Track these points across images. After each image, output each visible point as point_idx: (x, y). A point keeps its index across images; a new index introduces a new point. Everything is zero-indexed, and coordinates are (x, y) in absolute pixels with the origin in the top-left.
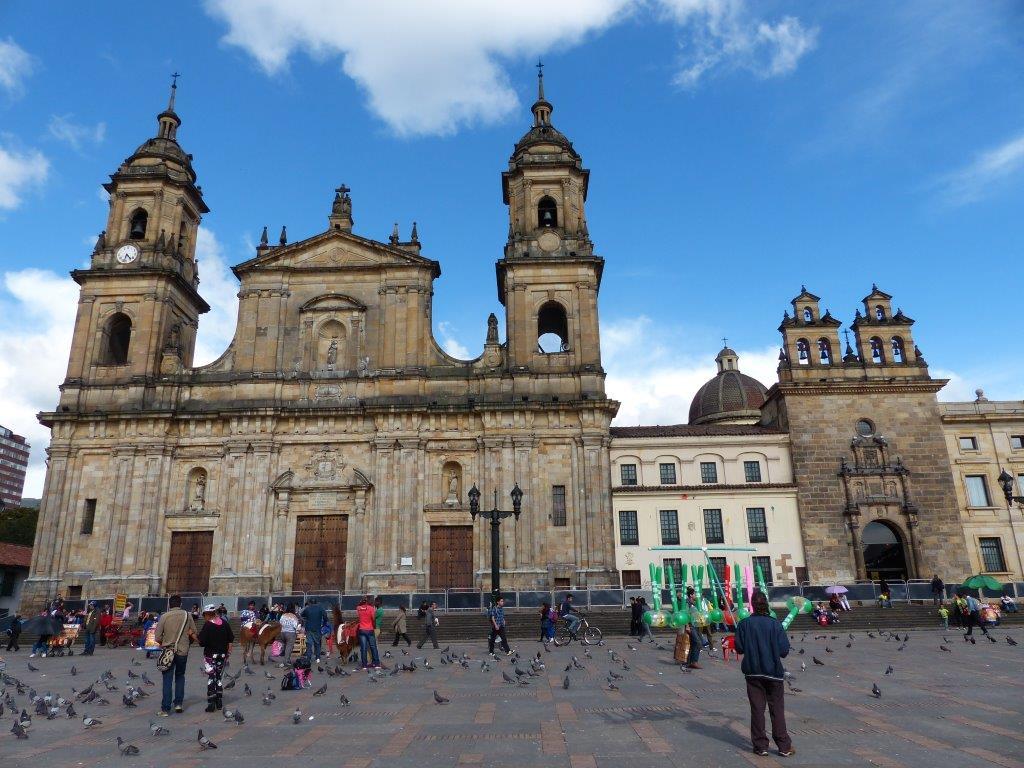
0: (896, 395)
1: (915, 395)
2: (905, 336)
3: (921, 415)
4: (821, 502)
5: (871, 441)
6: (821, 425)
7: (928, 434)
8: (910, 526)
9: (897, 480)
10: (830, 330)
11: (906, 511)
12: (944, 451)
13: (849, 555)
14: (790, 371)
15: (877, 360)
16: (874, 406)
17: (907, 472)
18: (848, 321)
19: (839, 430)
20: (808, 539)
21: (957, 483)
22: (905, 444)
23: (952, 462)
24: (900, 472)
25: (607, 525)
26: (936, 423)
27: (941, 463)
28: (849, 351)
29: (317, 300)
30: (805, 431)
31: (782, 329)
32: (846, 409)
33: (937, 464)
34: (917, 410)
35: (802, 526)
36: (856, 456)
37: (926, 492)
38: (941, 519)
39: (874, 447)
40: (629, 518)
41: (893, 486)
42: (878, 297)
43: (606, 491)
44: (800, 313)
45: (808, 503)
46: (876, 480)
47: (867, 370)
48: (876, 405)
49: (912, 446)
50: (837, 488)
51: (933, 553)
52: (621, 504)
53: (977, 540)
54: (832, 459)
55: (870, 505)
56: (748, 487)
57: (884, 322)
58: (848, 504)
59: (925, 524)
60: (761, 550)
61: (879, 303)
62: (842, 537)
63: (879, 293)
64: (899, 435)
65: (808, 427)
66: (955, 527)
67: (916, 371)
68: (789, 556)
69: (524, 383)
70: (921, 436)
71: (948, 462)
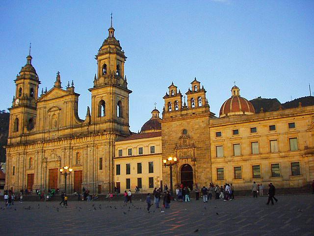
11: (194, 160)
24: (194, 146)
27: (207, 142)
28: (185, 104)
29: (51, 109)
40: (118, 166)
41: (191, 152)
46: (185, 150)
52: (117, 162)
59: (199, 165)
60: (151, 175)
64: (195, 134)
68: (158, 177)
69: (92, 128)
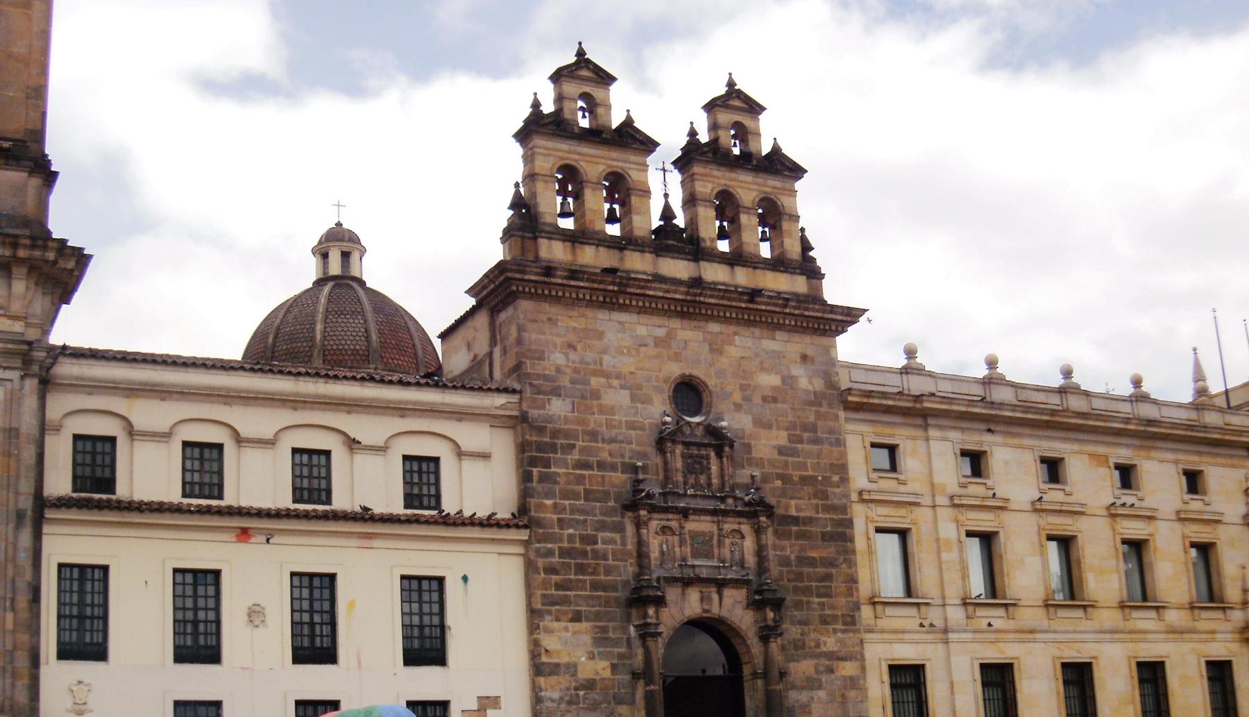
0: (757, 331)
1: (797, 337)
2: (784, 201)
3: (804, 383)
4: (581, 569)
5: (699, 431)
6: (595, 382)
7: (813, 429)
8: (767, 634)
9: (746, 528)
10: (633, 158)
12: (841, 468)
13: (632, 703)
14: (535, 238)
15: (723, 246)
16: (712, 350)
17: (769, 510)
18: (672, 142)
19: (634, 398)
20: (544, 659)
21: (860, 543)
22: (767, 444)
23: (854, 497)
25: (23, 600)
26: (830, 405)
28: (667, 214)
30: (557, 392)
31: (523, 136)
32: (651, 350)
33: (827, 498)
34: (798, 371)
35: (533, 628)
36: (666, 463)
37: (802, 560)
38: (824, 621)
39: (706, 446)
42: (737, 103)
43: (26, 503)
44: (567, 105)
45: (551, 570)
47: (703, 264)
48: (716, 350)
49: (781, 451)
50: (617, 536)
51: (803, 697)
53: (885, 670)
54: (613, 468)
55: (687, 583)
56: (409, 521)
57: (748, 161)
58: (638, 576)
61: (737, 117)
62: (621, 656)
63: (740, 95)
64: (758, 423)
65: (565, 381)
66: (850, 638)
67: (799, 284)
70: (803, 432)
71: (847, 496)
